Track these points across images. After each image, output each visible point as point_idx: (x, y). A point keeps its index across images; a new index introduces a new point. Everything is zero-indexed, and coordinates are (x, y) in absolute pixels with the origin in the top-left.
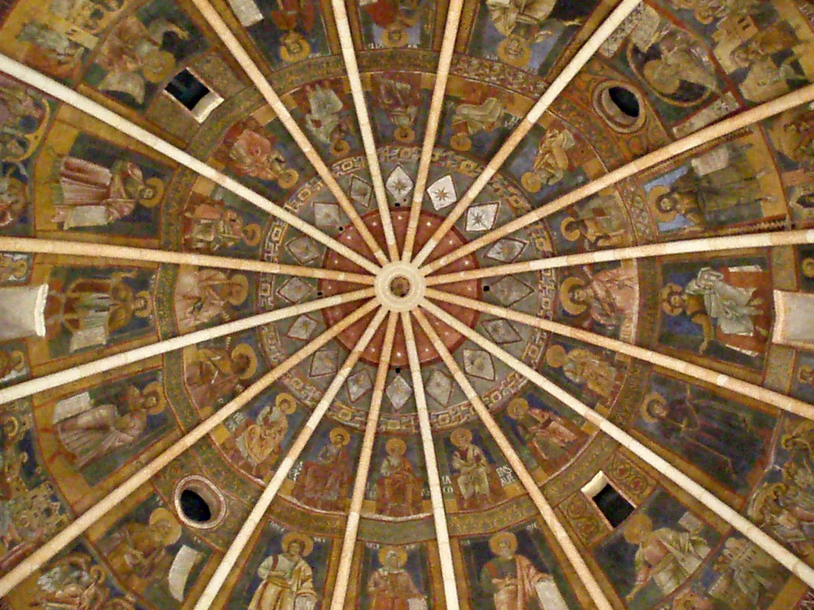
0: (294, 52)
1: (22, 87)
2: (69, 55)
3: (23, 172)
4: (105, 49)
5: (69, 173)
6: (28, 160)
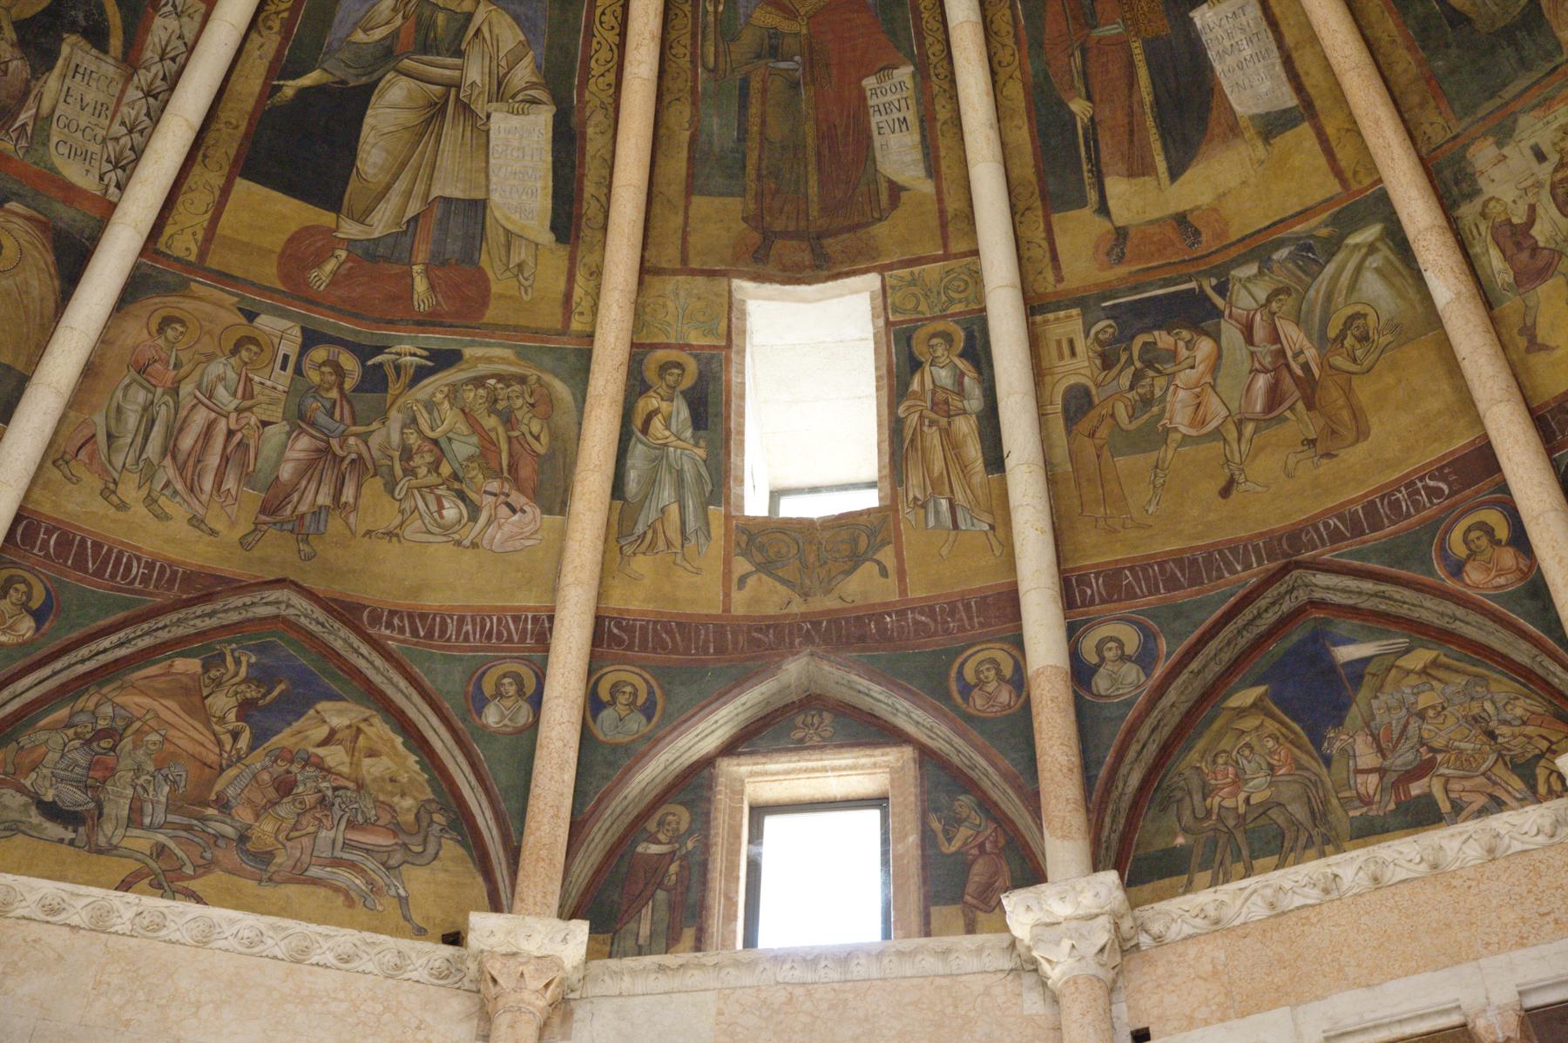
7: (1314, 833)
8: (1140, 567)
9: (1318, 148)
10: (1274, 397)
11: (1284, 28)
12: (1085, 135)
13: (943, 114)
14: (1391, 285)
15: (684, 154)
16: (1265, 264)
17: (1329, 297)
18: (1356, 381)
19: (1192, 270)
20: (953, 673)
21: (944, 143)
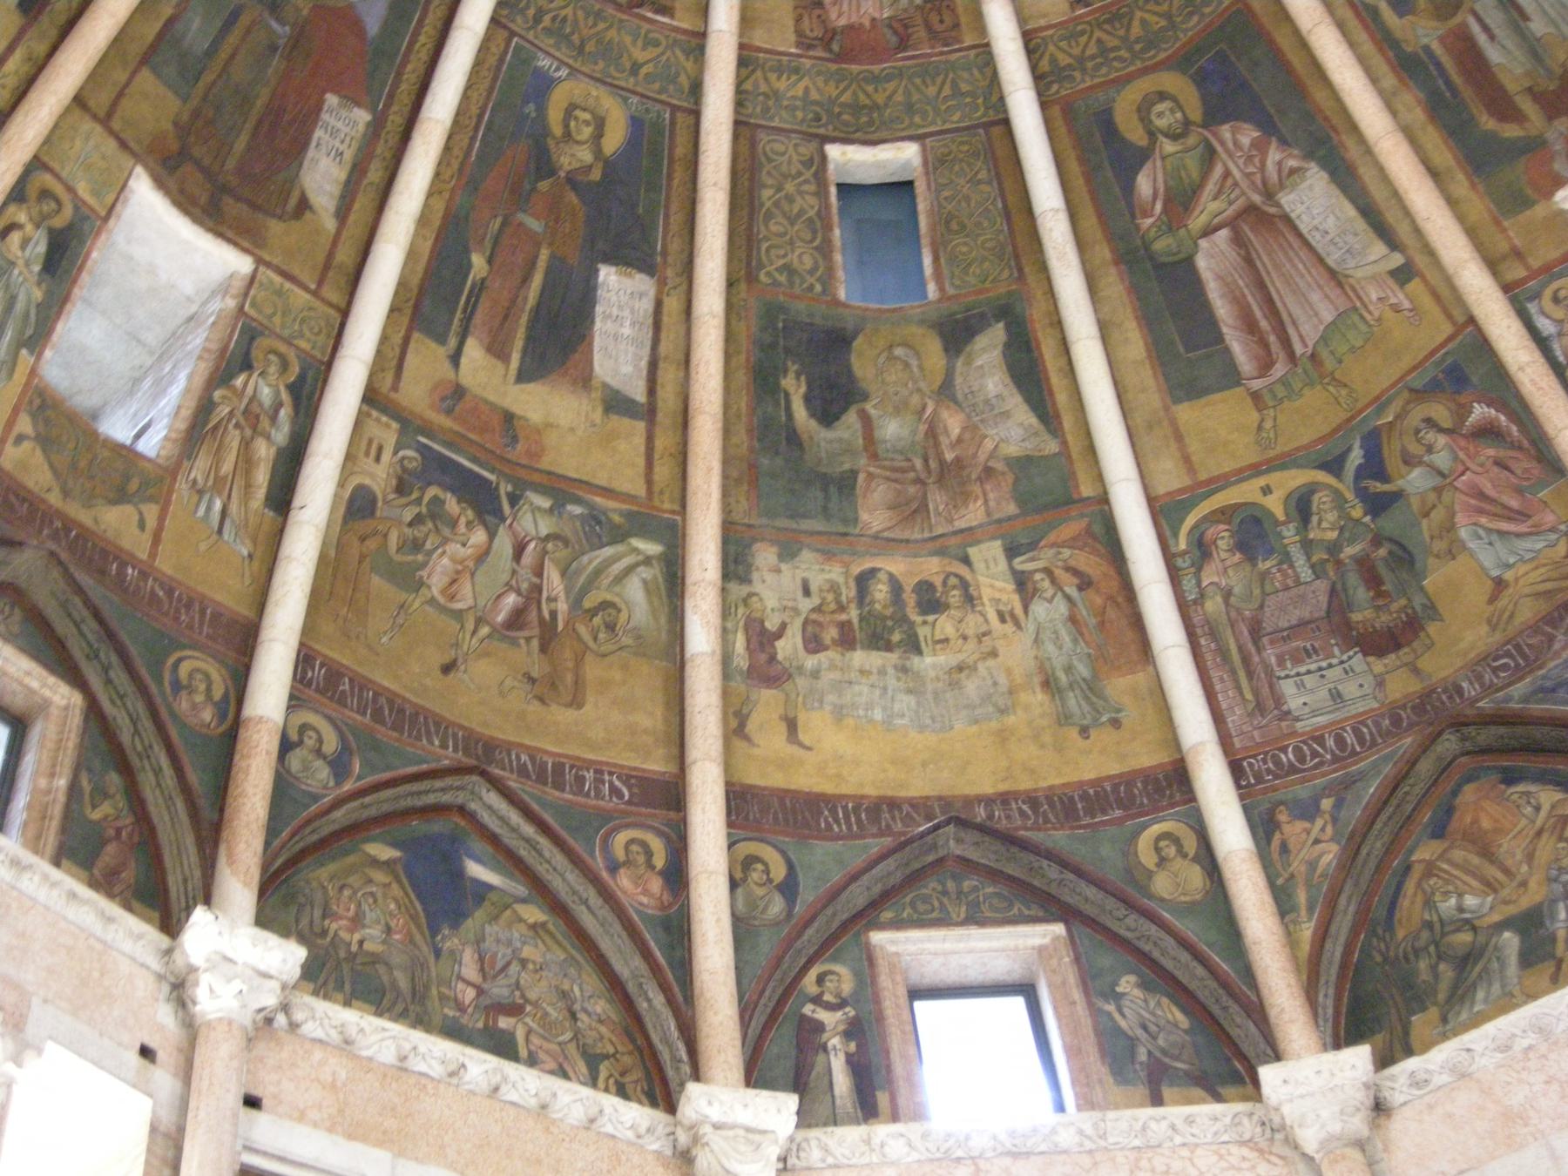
0: (591, 119)
1: (1196, 620)
2: (1053, 581)
3: (1356, 457)
4: (973, 515)
5: (1275, 346)
6: (1325, 466)
7: (411, 1008)
8: (360, 684)
9: (642, 449)
10: (516, 620)
11: (663, 335)
12: (471, 292)
13: (375, 174)
14: (650, 603)
15: (158, 25)
16: (556, 509)
17: (598, 572)
18: (589, 658)
19: (498, 466)
20: (171, 660)
21: (363, 203)
